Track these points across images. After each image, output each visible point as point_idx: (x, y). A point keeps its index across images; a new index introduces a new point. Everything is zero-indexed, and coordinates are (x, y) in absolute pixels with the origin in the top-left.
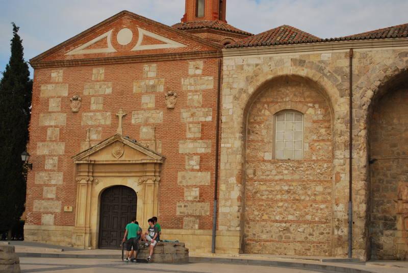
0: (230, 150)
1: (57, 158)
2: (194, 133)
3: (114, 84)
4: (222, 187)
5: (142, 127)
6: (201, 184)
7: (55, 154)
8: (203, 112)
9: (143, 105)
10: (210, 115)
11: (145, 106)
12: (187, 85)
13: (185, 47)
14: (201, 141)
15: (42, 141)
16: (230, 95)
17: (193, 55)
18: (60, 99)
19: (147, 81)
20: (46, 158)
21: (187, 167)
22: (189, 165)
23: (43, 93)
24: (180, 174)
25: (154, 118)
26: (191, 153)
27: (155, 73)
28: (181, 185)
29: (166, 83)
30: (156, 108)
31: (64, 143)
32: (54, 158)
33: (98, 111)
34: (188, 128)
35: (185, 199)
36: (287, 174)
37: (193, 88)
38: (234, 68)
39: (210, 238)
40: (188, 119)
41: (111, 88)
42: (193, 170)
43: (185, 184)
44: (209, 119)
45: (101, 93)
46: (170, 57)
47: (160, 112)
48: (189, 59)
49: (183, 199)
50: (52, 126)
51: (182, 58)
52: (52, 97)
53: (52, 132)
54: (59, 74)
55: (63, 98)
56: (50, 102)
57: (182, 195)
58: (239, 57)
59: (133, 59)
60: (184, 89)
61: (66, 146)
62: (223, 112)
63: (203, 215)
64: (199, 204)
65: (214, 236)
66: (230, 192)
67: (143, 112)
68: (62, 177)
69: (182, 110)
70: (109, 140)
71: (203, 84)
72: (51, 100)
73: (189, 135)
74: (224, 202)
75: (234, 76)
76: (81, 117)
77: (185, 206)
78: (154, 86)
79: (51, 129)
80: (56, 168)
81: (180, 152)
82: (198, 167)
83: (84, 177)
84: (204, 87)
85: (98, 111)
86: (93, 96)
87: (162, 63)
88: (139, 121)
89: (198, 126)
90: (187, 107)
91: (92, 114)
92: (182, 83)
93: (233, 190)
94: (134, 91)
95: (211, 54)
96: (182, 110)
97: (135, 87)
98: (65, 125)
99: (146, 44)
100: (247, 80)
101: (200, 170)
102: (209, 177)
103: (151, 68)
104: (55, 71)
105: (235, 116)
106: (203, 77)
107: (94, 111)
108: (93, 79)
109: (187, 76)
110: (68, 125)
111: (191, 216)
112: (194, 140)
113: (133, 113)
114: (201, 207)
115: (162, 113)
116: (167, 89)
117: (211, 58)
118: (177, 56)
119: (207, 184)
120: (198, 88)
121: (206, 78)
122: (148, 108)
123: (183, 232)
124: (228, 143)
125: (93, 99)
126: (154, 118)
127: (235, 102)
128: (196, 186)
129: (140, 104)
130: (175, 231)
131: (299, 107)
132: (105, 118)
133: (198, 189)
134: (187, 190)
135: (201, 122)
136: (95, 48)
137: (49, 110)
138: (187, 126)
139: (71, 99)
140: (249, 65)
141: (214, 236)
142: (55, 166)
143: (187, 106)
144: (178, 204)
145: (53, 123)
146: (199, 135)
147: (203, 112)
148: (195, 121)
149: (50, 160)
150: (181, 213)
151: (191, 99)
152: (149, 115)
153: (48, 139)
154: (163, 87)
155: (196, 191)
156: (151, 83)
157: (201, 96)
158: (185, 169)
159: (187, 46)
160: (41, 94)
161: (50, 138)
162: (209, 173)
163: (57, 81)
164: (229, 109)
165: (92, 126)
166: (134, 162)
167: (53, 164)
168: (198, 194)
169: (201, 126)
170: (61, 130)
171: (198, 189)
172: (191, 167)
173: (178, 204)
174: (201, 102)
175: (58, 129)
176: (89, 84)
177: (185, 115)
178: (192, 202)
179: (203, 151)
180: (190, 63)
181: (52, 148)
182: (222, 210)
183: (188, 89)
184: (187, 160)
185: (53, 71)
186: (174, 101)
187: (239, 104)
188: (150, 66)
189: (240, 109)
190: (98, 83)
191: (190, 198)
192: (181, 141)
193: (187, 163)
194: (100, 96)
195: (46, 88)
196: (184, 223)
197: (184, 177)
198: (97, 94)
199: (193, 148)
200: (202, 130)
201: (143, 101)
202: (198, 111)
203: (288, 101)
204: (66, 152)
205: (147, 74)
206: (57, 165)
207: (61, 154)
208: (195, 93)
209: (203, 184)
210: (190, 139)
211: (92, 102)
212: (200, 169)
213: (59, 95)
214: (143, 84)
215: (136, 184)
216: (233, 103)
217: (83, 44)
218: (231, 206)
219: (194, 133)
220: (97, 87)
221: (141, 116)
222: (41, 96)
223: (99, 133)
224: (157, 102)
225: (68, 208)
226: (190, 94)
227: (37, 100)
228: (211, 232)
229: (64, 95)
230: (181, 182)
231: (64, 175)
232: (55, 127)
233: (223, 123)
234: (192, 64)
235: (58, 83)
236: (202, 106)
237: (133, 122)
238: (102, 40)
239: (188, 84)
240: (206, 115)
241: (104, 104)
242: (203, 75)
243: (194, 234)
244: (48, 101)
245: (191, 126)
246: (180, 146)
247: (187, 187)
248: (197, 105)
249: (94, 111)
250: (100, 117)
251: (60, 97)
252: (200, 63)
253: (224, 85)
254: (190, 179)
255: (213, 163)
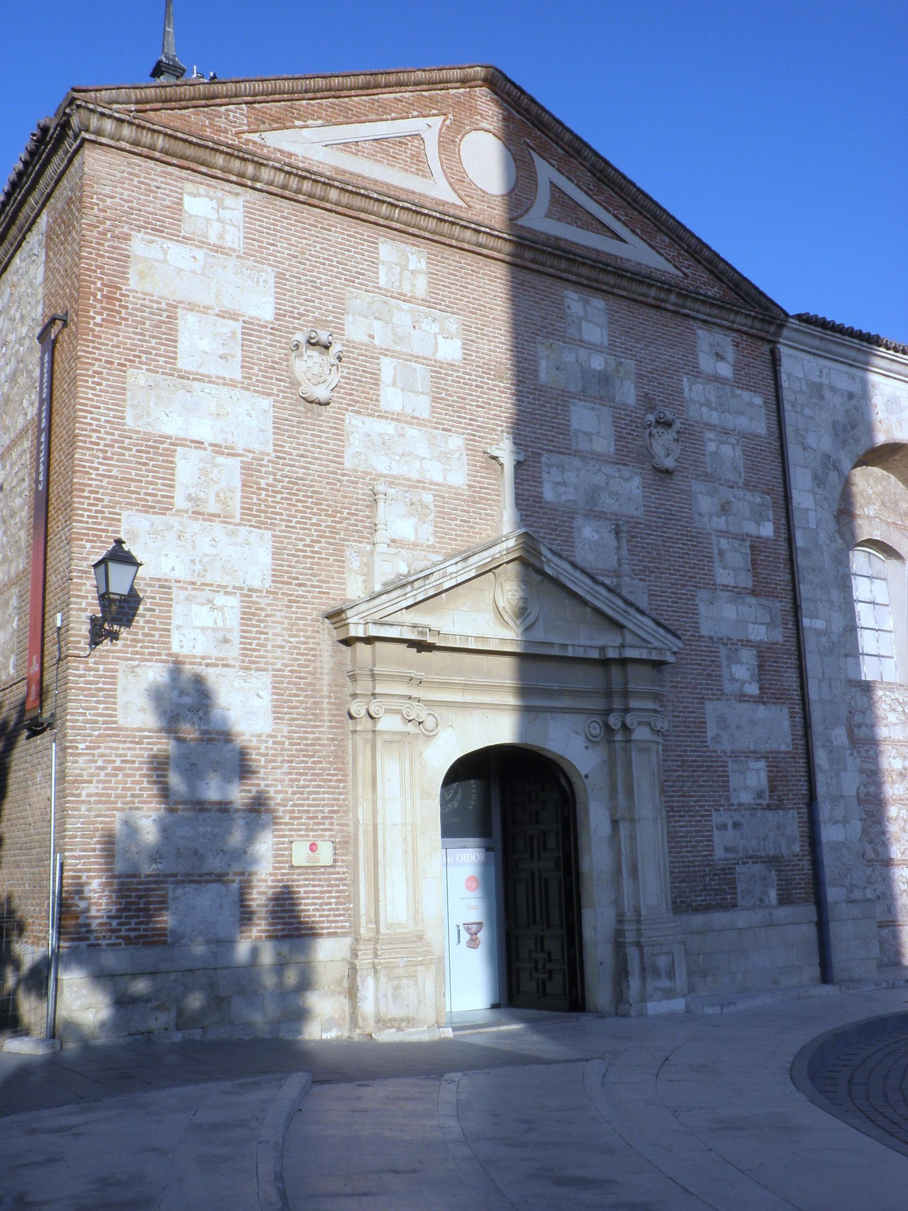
0: (824, 640)
1: (234, 602)
2: (735, 570)
3: (466, 329)
4: (821, 757)
5: (579, 521)
6: (768, 747)
7: (226, 580)
8: (750, 503)
9: (576, 436)
10: (769, 520)
11: (584, 446)
12: (702, 405)
13: (677, 276)
14: (753, 600)
15: (147, 509)
16: (806, 467)
17: (716, 312)
18: (237, 326)
19: (583, 353)
20: (178, 595)
21: (728, 688)
22: (733, 679)
23: (141, 275)
24: (711, 709)
25: (614, 495)
26: (735, 637)
27: (605, 333)
28: (718, 748)
29: (640, 376)
30: (620, 460)
31: (268, 534)
32: (220, 600)
33: (414, 421)
34: (716, 551)
35: (734, 801)
36: (895, 725)
37: (714, 418)
38: (804, 388)
39: (810, 932)
40: (715, 518)
41: (458, 343)
42: (743, 698)
43: (727, 746)
44: (767, 530)
45: (418, 347)
46: (653, 292)
47: (628, 479)
48: (695, 319)
49: (728, 798)
50: (198, 444)
51: (683, 311)
52: (192, 307)
53: (204, 472)
54: (225, 214)
55: (250, 327)
56: (180, 322)
57: (725, 786)
58: (811, 358)
59: (541, 258)
60: (693, 412)
61: (277, 553)
62: (797, 518)
63: (785, 853)
64: (770, 815)
65: (822, 926)
66: (838, 775)
67: (577, 462)
68: (267, 695)
69: (697, 486)
70: (496, 549)
71: (742, 414)
72: (188, 322)
73: (724, 577)
74: (829, 807)
75: (807, 411)
76: (339, 433)
77: (736, 825)
78: (605, 379)
79: (195, 454)
80: (234, 651)
81: (704, 632)
82: (753, 689)
83: (395, 704)
84: (742, 423)
85: (414, 421)
86: (386, 352)
87: (623, 303)
88: (568, 495)
89: (744, 551)
90: (708, 477)
91: (389, 428)
92: (686, 394)
93: (845, 769)
94: (543, 376)
95: (757, 324)
96: (697, 486)
97: (543, 364)
98: (270, 449)
99: (558, 220)
100: (836, 434)
101: (760, 700)
102: (786, 724)
103: (590, 310)
104: (202, 189)
105: (823, 537)
106: (738, 392)
107: (396, 418)
108: (382, 282)
109: (697, 373)
110: (280, 454)
111: (755, 859)
112: (737, 593)
113: (543, 459)
114: (778, 827)
115: (636, 481)
116: (648, 402)
117: (753, 336)
118: (673, 298)
119: (783, 748)
120: (731, 421)
121: (746, 395)
122: (593, 452)
123: (740, 919)
124: (817, 617)
125: (387, 368)
126: (614, 495)
127: (817, 490)
128: (757, 755)
129: (565, 431)
130: (719, 918)
131: (893, 539)
132: (444, 457)
133: (762, 764)
134: (735, 767)
135: (748, 535)
136: (371, 156)
137: (180, 364)
138: (714, 540)
139: (300, 337)
140: (834, 390)
141: (822, 926)
142: (226, 641)
143: (706, 475)
144: (717, 819)
145: (203, 430)
146: (746, 580)
147: (750, 503)
148: (731, 529)
149: (195, 608)
150: (727, 850)
151: (716, 453)
152: (599, 479)
153: (180, 502)
154: (632, 391)
155: (758, 771)
156: (597, 363)
157: (739, 451)
158: (723, 694)
159: (681, 274)
160: (132, 274)
161: (190, 498)
162: (786, 710)
163: (213, 239)
164: (807, 510)
165: (392, 481)
166: (580, 653)
167: (215, 630)
168: (764, 781)
169: (749, 551)
170: (247, 469)
171: (762, 764)
172: (737, 685)
173: (717, 819)
174: (742, 469)
175: (235, 463)
176: (368, 297)
177: (705, 504)
178: (752, 809)
179: (759, 633)
180: (700, 332)
181: (208, 550)
182: (829, 834)
183: (705, 419)
184: (724, 662)
185: (189, 187)
186: (673, 446)
187: (826, 499)
188: (586, 302)
189: (832, 517)
190: (406, 306)
191: (746, 797)
192: (703, 594)
193: (725, 672)
194: (417, 358)
195: (153, 252)
196: (739, 885)
197: (722, 721)
198: (397, 348)
199: (738, 621)
200: (754, 563)
201: (575, 424)
202: (735, 497)
203: (875, 517)
204: (276, 577)
205: (580, 329)
206: (235, 637)
207: (256, 584)
208: (724, 438)
209: (774, 746)
210: (725, 588)
211: (386, 375)
212: (761, 696)
213: (228, 305)
214: (569, 357)
215: (579, 742)
216: (812, 491)
217: (328, 123)
218: (845, 821)
219: (735, 570)
220: (403, 316)
221: (571, 477)
222: (134, 282)
223: (422, 517)
224: (619, 438)
225: (313, 847)
226: (710, 435)
227: (109, 298)
228: (811, 911)
229: (253, 312)
230: (716, 738)
231: (277, 689)
232: (217, 449)
233: (799, 553)
234: (705, 338)
235: (218, 249)
236: (746, 485)
237: (548, 494)
238: (401, 141)
239: (703, 401)
240: (758, 518)
241: (435, 400)
242: (738, 383)
243: (770, 925)
244: (172, 317)
245: (724, 544)
246: (702, 608)
247: (736, 755)
248: (732, 477)
249: (396, 418)
250: (423, 450)
251: (232, 316)
252: (726, 342)
253: (789, 431)
254: (738, 727)
255: (791, 678)
